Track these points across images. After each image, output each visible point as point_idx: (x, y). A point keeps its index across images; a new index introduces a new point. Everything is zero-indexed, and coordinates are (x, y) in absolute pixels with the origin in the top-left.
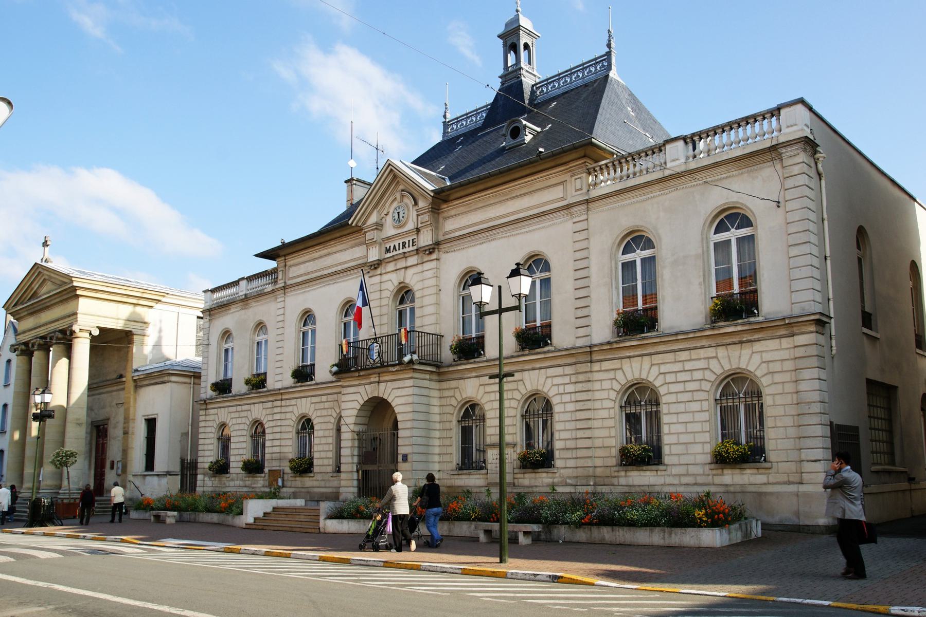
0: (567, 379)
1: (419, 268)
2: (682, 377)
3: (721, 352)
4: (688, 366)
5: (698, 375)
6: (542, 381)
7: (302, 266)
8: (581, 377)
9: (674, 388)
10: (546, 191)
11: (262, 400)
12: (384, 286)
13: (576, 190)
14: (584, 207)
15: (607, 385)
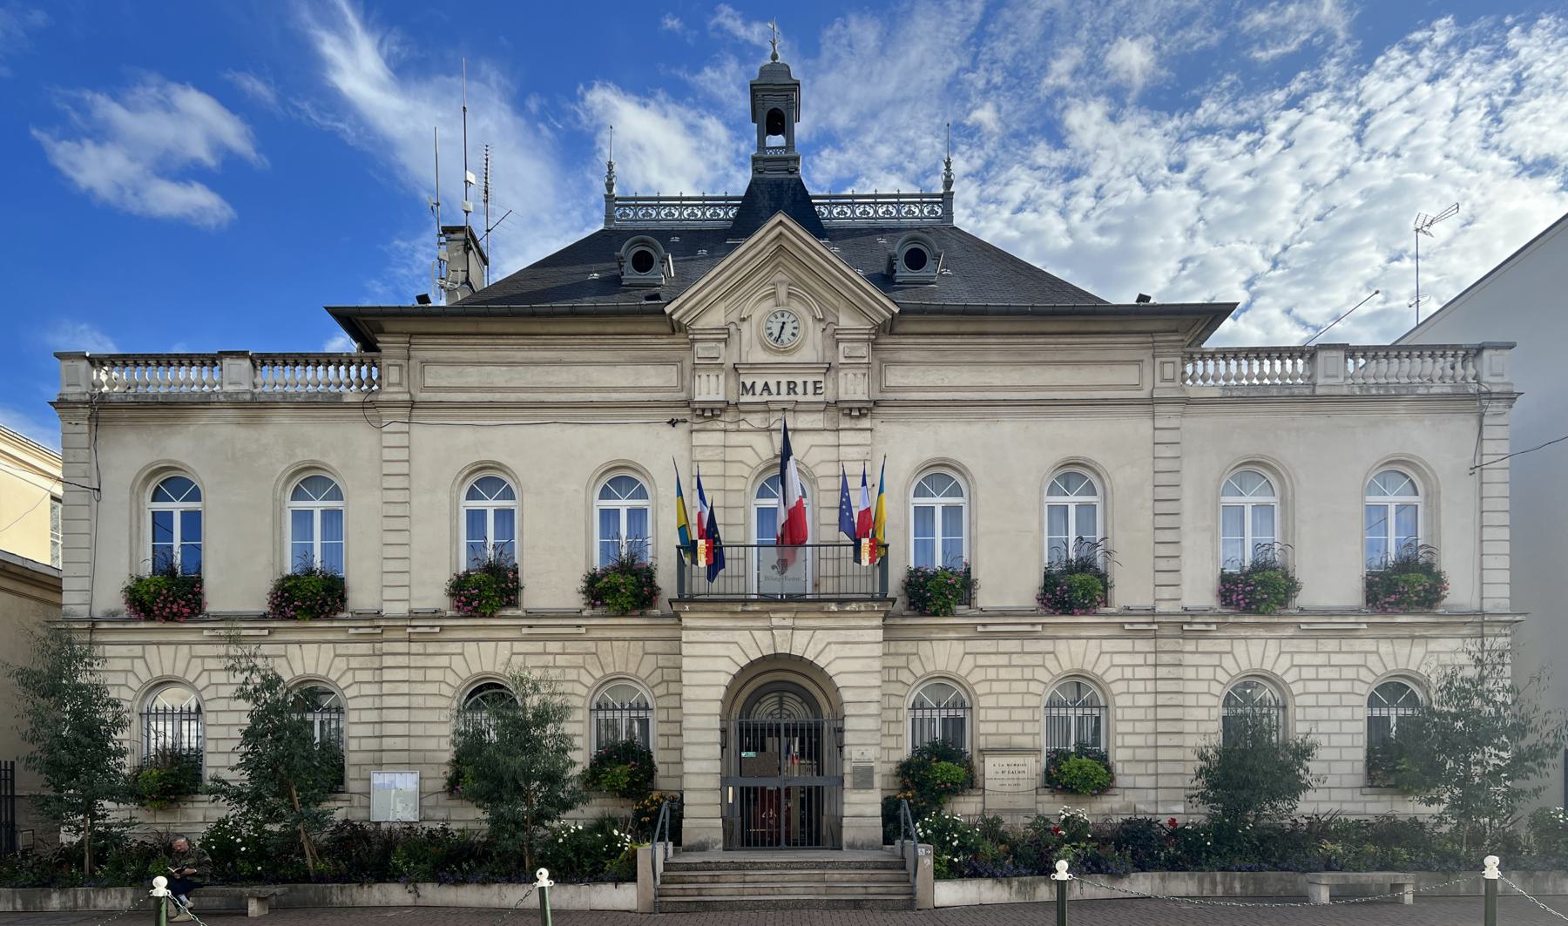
0: (1139, 659)
1: (830, 438)
2: (1325, 673)
3: (1385, 647)
4: (1336, 659)
5: (1349, 673)
6: (1092, 657)
7: (470, 369)
8: (1165, 658)
9: (1313, 687)
10: (1106, 368)
11: (330, 636)
12: (731, 455)
13: (1163, 380)
14: (1179, 408)
15: (1206, 673)
